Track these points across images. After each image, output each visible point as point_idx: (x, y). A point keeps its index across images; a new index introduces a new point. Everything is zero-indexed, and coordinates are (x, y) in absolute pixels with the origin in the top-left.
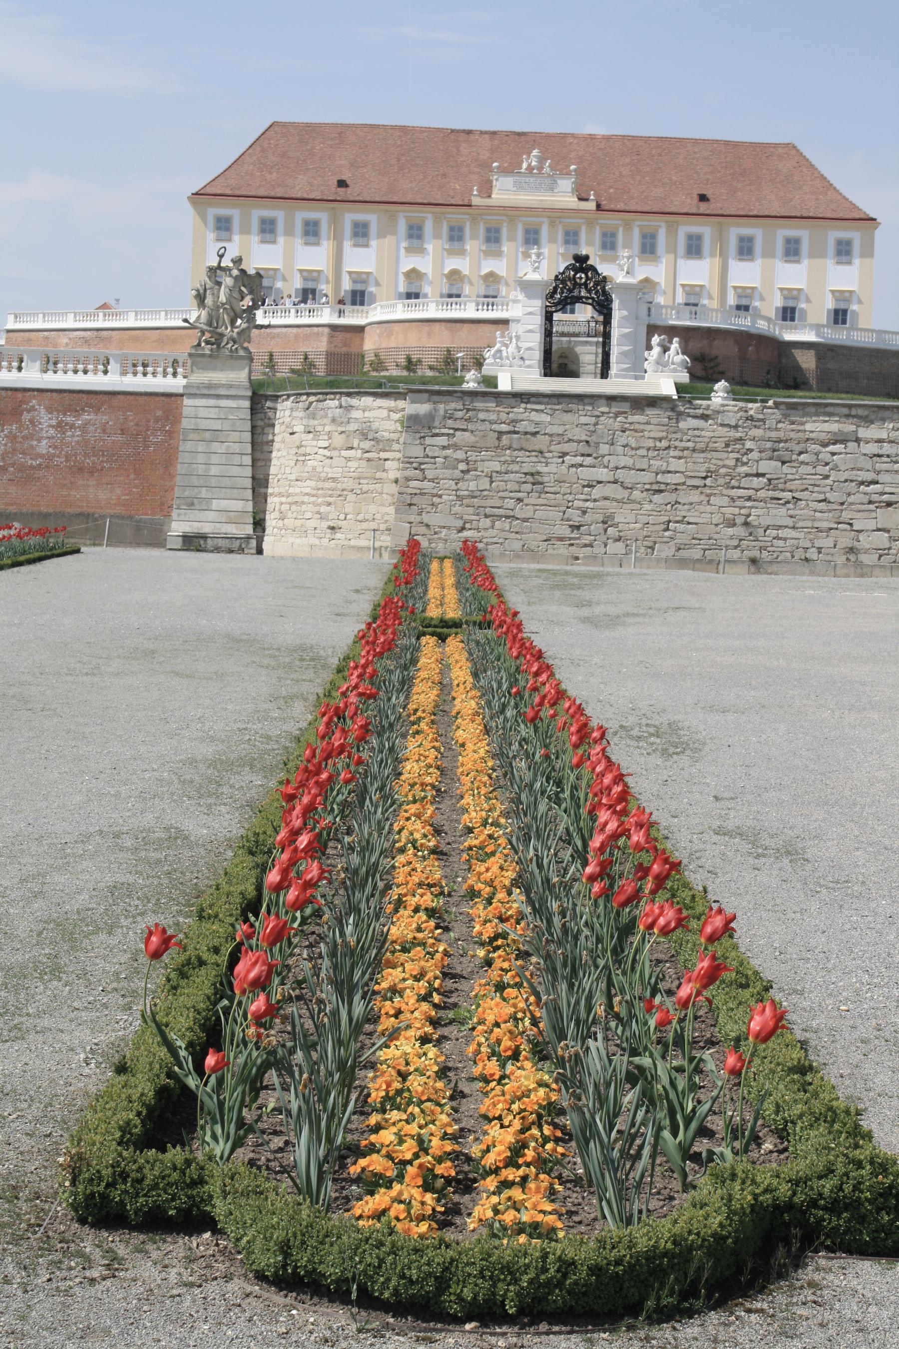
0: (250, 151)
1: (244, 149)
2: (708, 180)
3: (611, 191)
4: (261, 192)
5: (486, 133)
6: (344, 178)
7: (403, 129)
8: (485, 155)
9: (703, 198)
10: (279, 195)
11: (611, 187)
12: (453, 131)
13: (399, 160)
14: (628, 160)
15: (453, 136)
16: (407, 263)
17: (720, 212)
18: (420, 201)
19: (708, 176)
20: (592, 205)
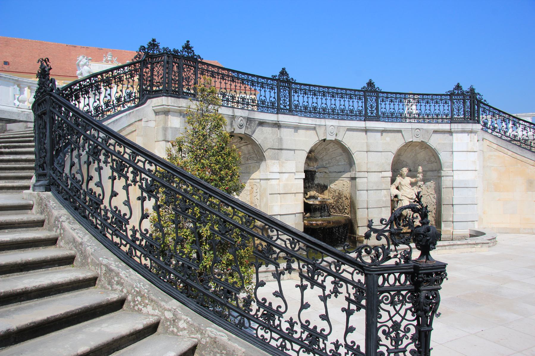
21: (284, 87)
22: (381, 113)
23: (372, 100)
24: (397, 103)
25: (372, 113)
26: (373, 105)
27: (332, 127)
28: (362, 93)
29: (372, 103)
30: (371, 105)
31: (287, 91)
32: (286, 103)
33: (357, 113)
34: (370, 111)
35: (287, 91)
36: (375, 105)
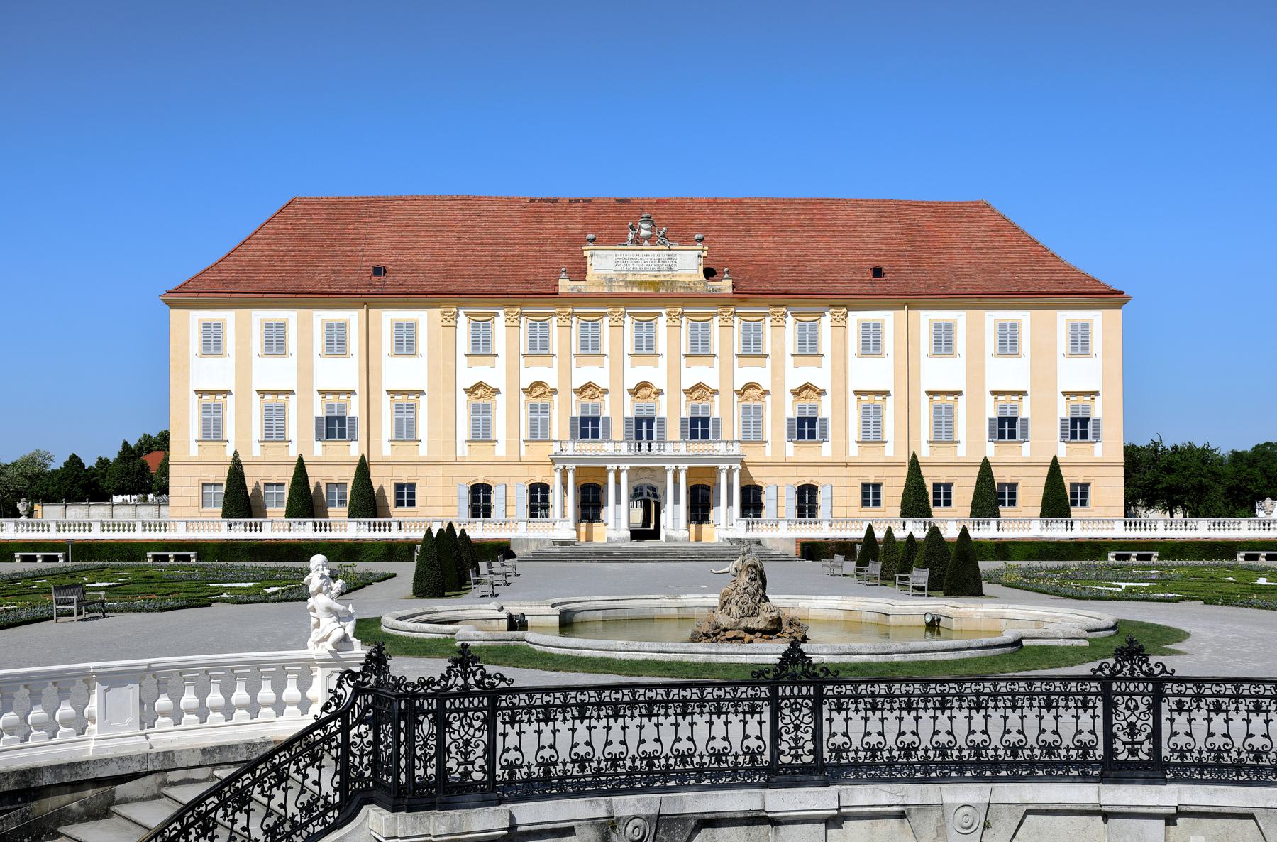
0: (259, 234)
1: (252, 231)
2: (880, 250)
3: (751, 268)
4: (266, 286)
5: (577, 201)
6: (382, 263)
7: (466, 201)
8: (575, 229)
9: (878, 272)
10: (289, 289)
11: (751, 264)
12: (532, 201)
13: (459, 238)
14: (769, 228)
15: (533, 207)
16: (468, 375)
17: (906, 290)
18: (487, 290)
19: (880, 245)
20: (725, 285)
21: (795, 698)
22: (1173, 751)
23: (1137, 707)
24: (1244, 715)
25: (1133, 752)
26: (1139, 724)
27: (966, 809)
28: (1095, 687)
29: (1133, 719)
30: (1132, 726)
31: (806, 711)
32: (802, 748)
33: (1073, 752)
34: (1124, 743)
35: (806, 711)
36: (1145, 723)
